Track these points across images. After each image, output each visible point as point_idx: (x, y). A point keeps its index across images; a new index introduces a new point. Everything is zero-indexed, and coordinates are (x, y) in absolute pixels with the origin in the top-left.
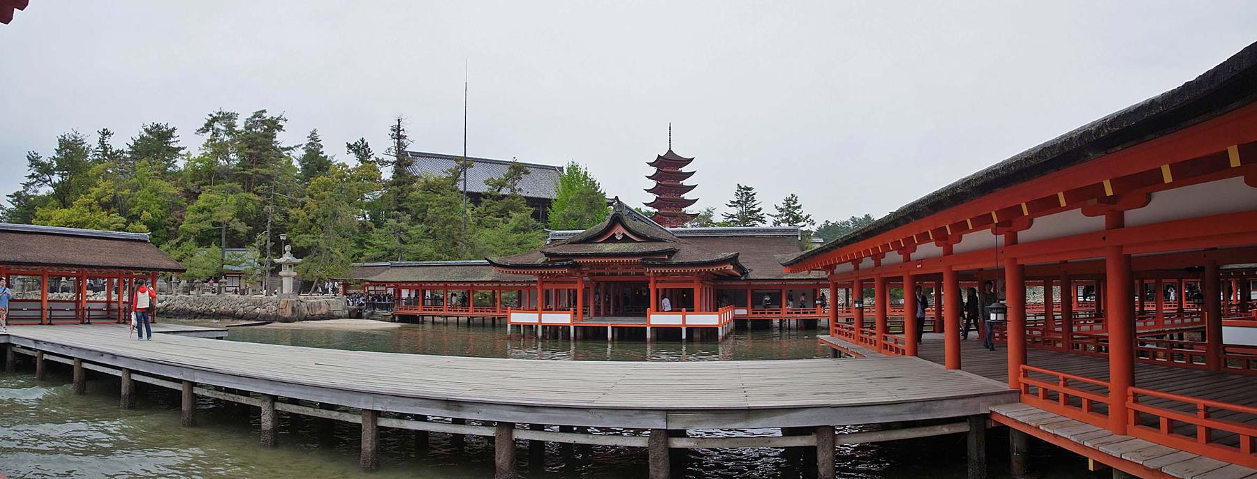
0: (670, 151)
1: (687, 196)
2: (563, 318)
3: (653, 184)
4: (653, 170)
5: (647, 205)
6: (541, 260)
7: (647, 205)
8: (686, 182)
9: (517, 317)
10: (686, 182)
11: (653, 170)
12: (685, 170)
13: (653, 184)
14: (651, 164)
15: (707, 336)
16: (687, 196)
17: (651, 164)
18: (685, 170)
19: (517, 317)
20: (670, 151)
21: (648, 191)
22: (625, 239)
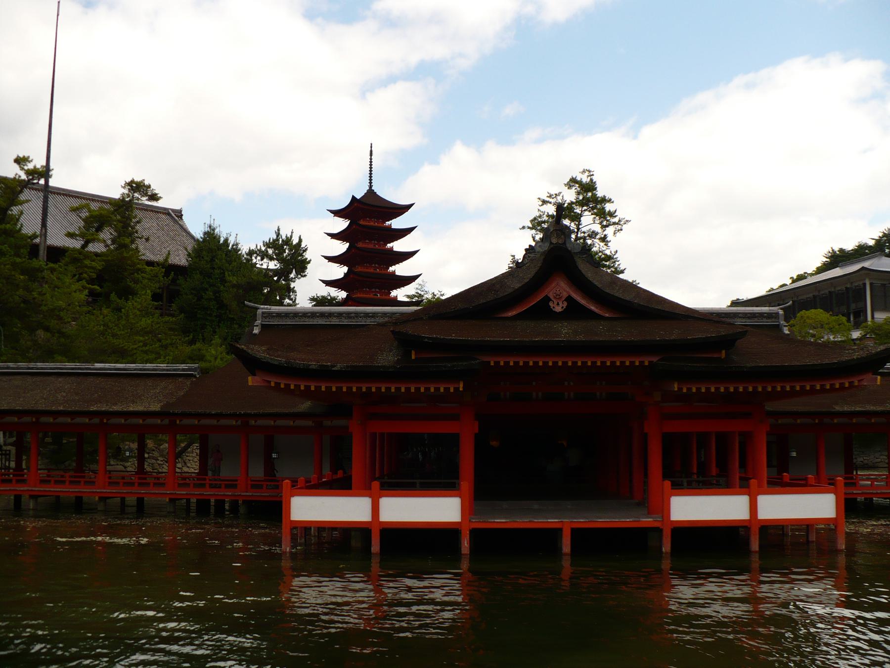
0: (371, 192)
1: (400, 269)
2: (443, 509)
3: (341, 247)
4: (342, 224)
5: (328, 283)
6: (388, 358)
7: (328, 283)
8: (398, 246)
9: (307, 508)
10: (398, 246)
11: (342, 224)
12: (396, 223)
13: (341, 247)
14: (337, 213)
15: (786, 547)
16: (400, 269)
17: (337, 213)
18: (396, 223)
19: (307, 508)
20: (371, 192)
21: (331, 259)
22: (574, 311)
